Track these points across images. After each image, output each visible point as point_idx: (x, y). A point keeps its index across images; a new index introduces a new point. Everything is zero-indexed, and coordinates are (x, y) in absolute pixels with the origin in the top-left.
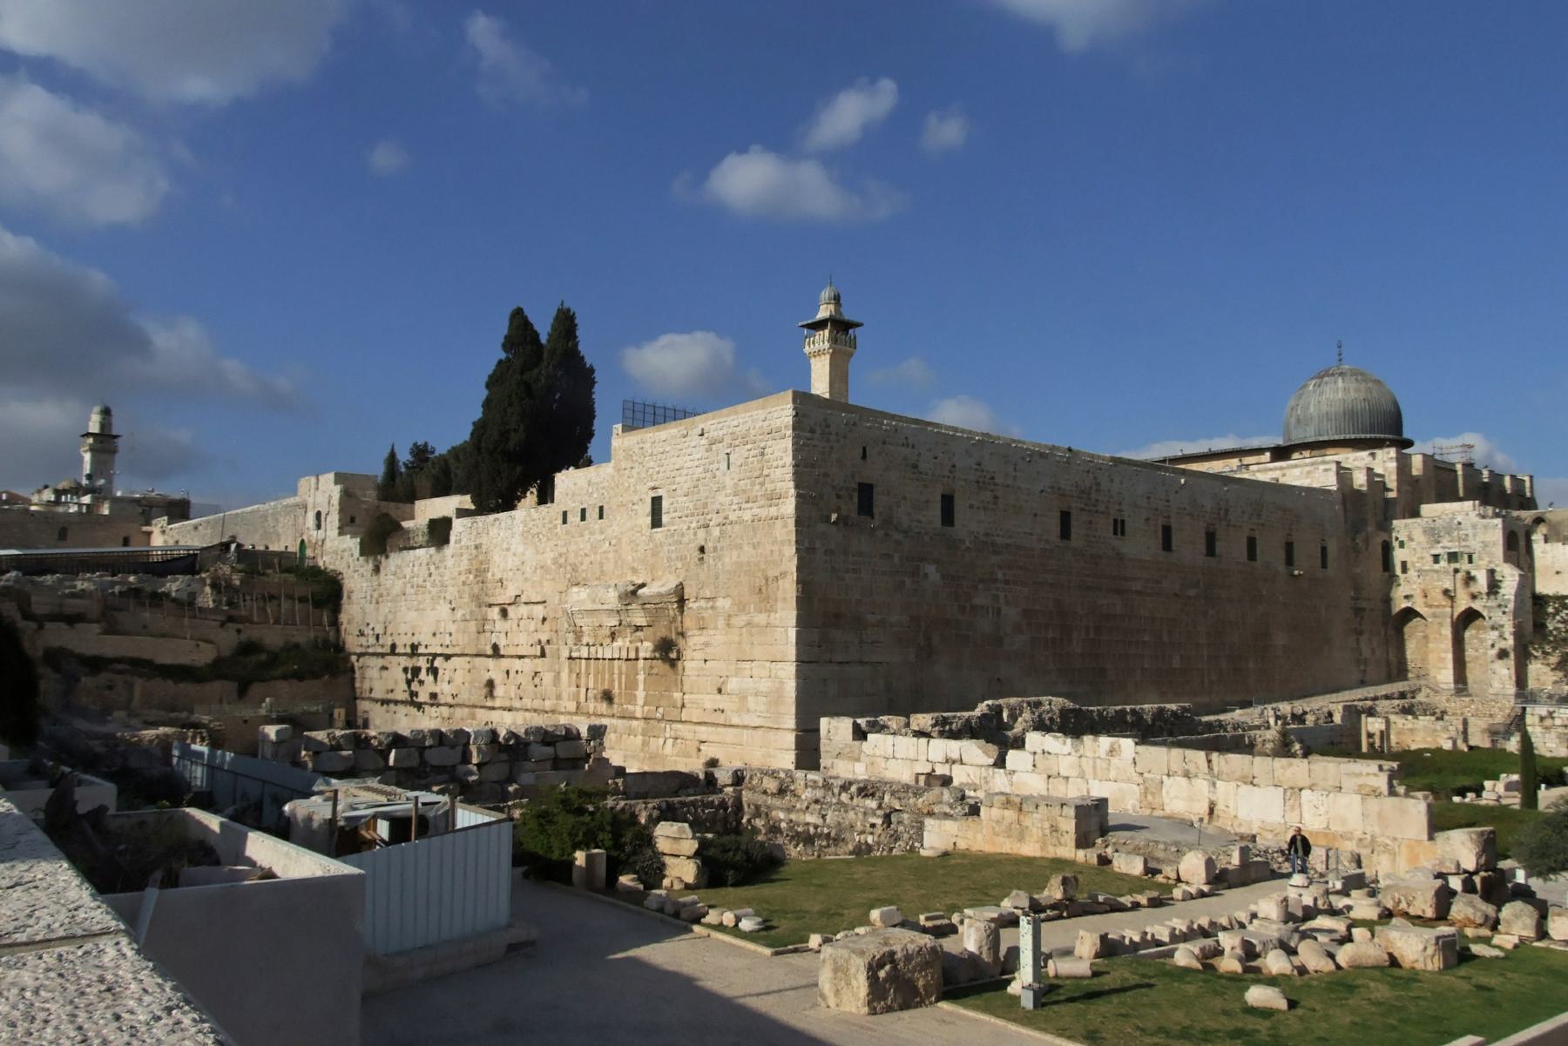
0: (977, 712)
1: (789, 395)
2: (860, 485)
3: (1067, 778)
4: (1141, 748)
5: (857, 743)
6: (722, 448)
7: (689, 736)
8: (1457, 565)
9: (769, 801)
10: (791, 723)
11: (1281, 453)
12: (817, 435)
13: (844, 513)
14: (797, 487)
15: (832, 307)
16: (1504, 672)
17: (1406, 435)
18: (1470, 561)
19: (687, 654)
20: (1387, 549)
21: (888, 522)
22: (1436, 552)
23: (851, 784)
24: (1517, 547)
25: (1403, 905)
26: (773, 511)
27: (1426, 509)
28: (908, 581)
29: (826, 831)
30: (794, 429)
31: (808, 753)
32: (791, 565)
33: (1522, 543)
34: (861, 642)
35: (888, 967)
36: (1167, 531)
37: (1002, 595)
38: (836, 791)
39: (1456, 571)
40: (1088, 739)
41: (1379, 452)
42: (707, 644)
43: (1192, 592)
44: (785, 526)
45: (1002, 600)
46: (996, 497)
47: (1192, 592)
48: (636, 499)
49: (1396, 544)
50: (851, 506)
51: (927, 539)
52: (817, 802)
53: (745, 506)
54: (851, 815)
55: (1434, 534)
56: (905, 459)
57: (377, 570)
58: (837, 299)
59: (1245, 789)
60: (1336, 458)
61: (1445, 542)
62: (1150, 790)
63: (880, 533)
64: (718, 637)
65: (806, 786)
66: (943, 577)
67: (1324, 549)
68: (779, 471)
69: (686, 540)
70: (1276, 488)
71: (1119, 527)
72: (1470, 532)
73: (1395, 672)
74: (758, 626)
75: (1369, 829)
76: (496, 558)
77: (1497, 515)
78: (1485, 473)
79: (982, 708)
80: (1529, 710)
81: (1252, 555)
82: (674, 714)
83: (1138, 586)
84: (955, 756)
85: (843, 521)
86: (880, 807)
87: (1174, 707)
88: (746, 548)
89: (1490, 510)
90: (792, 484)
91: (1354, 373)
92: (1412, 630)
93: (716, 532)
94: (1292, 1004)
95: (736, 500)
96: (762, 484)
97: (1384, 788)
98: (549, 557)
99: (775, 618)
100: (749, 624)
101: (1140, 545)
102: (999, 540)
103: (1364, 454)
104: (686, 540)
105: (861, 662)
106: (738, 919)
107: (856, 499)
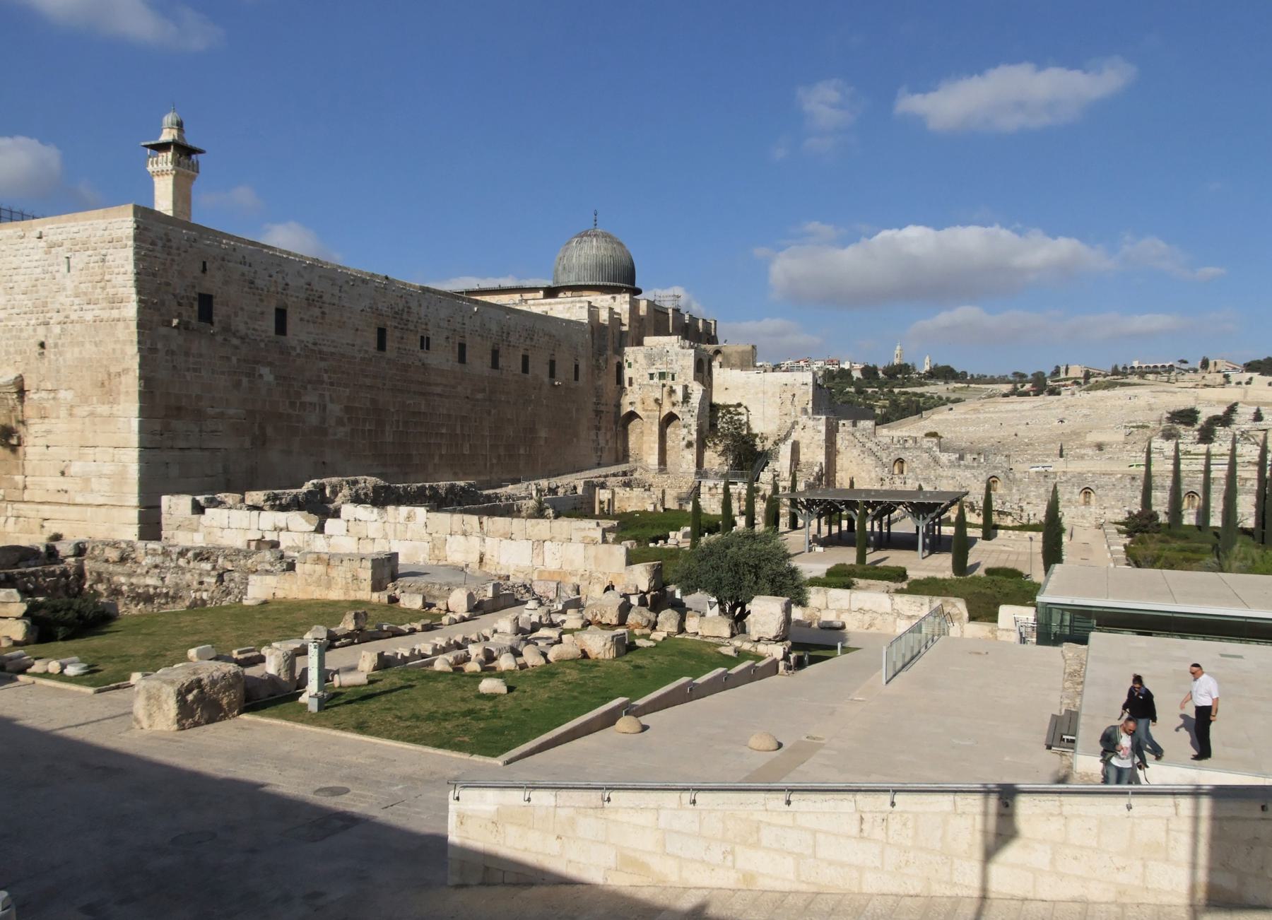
0: (304, 489)
1: (129, 209)
2: (200, 295)
3: (374, 539)
4: (432, 515)
5: (196, 516)
6: (62, 252)
7: (32, 514)
9: (111, 568)
10: (134, 500)
11: (551, 292)
12: (158, 248)
13: (185, 318)
14: (138, 293)
15: (175, 132)
16: (690, 456)
17: (637, 285)
19: (29, 440)
20: (620, 368)
21: (226, 329)
23: (188, 550)
24: (703, 370)
25: (598, 617)
27: (648, 340)
28: (245, 380)
29: (165, 590)
30: (135, 240)
31: (150, 526)
32: (132, 361)
33: (706, 367)
34: (201, 431)
35: (195, 692)
36: (462, 347)
37: (327, 394)
38: (174, 557)
39: (664, 386)
40: (390, 509)
41: (618, 296)
42: (49, 432)
43: (480, 396)
44: (127, 327)
45: (327, 399)
46: (323, 313)
47: (480, 396)
49: (626, 365)
50: (192, 314)
51: (262, 345)
52: (156, 566)
53: (85, 307)
54: (188, 576)
55: (651, 359)
56: (243, 274)
58: (180, 125)
59: (505, 542)
60: (589, 299)
61: (658, 365)
62: (436, 545)
63: (219, 338)
64: (60, 425)
65: (146, 554)
66: (276, 378)
67: (577, 367)
68: (120, 278)
69: (25, 335)
70: (545, 318)
71: (425, 343)
72: (674, 358)
73: (621, 456)
74: (101, 416)
75: (588, 568)
77: (691, 347)
78: (687, 317)
79: (308, 486)
81: (525, 369)
82: (16, 495)
83: (438, 390)
84: (283, 525)
85: (184, 326)
86: (214, 568)
87: (462, 483)
88: (88, 346)
89: (687, 343)
90: (133, 290)
91: (606, 236)
92: (634, 426)
93: (57, 330)
94: (510, 689)
95: (77, 301)
96: (103, 288)
97: (600, 539)
99: (116, 409)
100: (92, 414)
101: (441, 357)
102: (325, 349)
103: (608, 297)
104: (25, 335)
105: (201, 449)
106: (63, 667)
107: (196, 307)
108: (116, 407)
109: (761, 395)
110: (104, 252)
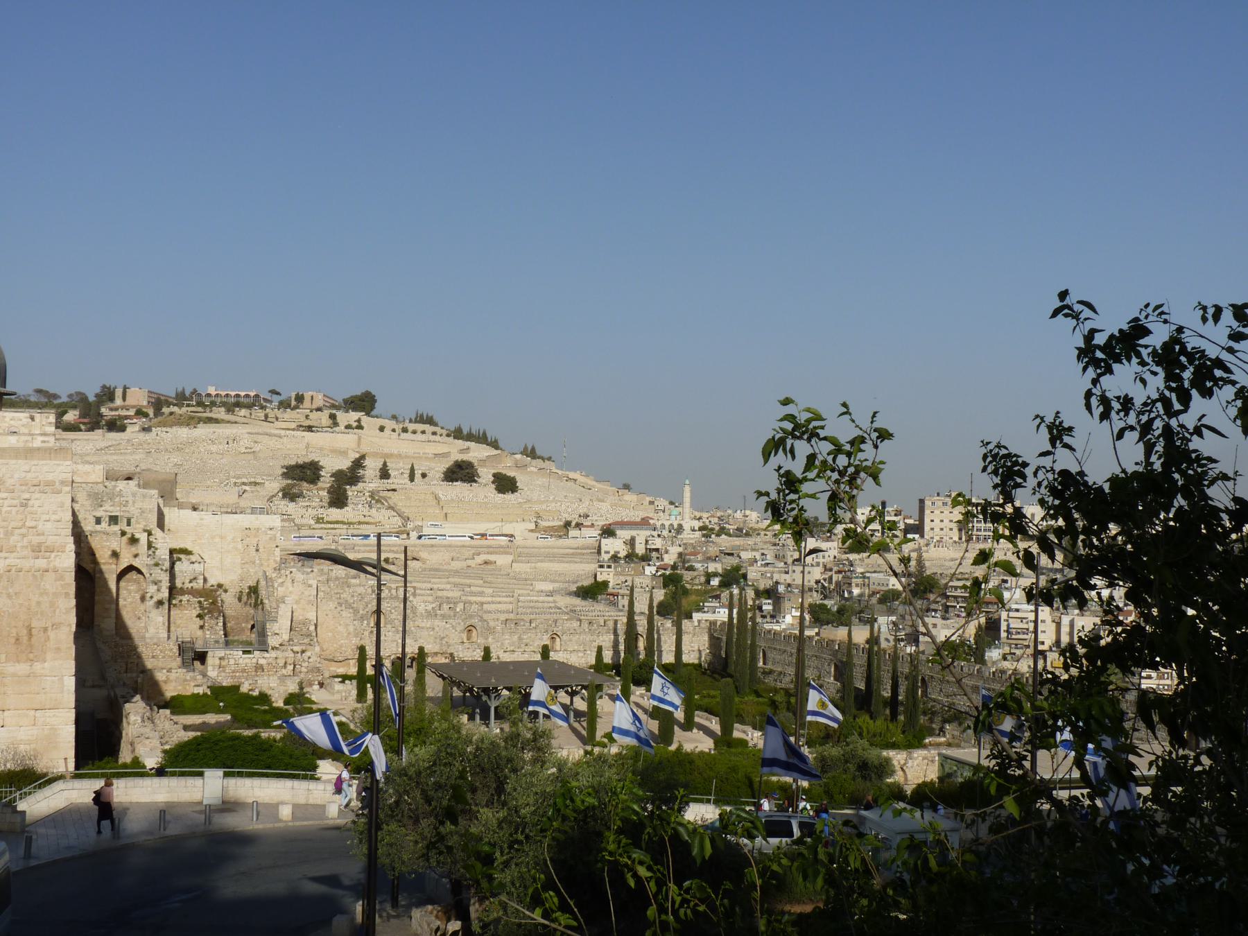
8: (116, 528)
18: (129, 524)
22: (98, 515)
26: (41, 563)
61: (107, 506)
72: (130, 499)
74: (14, 675)
80: (210, 654)
108: (38, 666)
109: (217, 540)
110: (27, 496)
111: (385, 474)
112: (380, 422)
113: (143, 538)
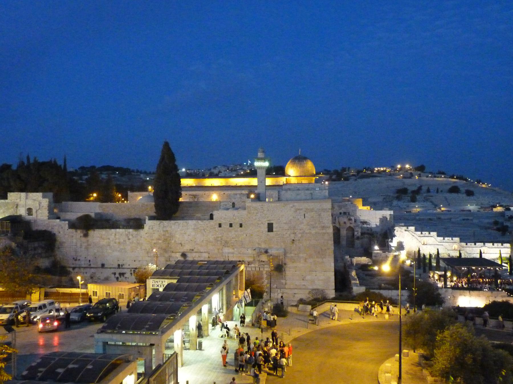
22: (341, 211)
26: (324, 231)
48: (260, 223)
57: (86, 235)
76: (177, 236)
93: (300, 235)
98: (211, 238)
111: (428, 191)
112: (427, 174)
113: (353, 218)
